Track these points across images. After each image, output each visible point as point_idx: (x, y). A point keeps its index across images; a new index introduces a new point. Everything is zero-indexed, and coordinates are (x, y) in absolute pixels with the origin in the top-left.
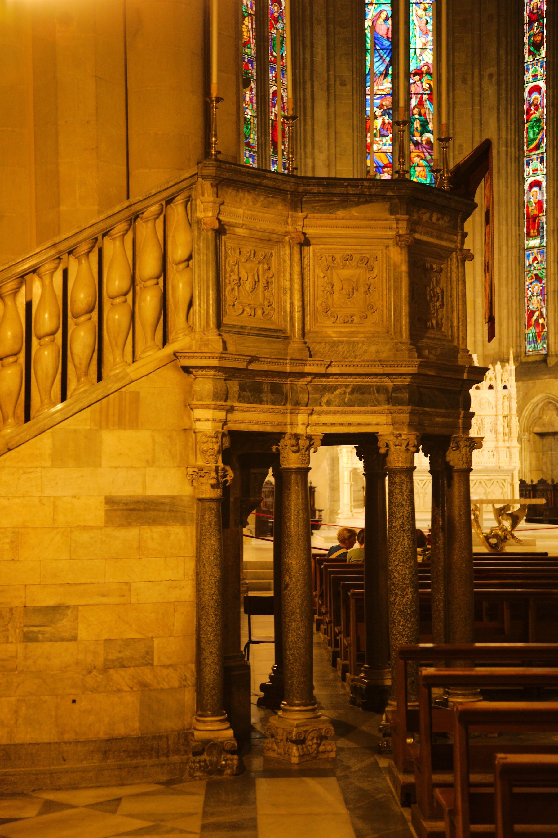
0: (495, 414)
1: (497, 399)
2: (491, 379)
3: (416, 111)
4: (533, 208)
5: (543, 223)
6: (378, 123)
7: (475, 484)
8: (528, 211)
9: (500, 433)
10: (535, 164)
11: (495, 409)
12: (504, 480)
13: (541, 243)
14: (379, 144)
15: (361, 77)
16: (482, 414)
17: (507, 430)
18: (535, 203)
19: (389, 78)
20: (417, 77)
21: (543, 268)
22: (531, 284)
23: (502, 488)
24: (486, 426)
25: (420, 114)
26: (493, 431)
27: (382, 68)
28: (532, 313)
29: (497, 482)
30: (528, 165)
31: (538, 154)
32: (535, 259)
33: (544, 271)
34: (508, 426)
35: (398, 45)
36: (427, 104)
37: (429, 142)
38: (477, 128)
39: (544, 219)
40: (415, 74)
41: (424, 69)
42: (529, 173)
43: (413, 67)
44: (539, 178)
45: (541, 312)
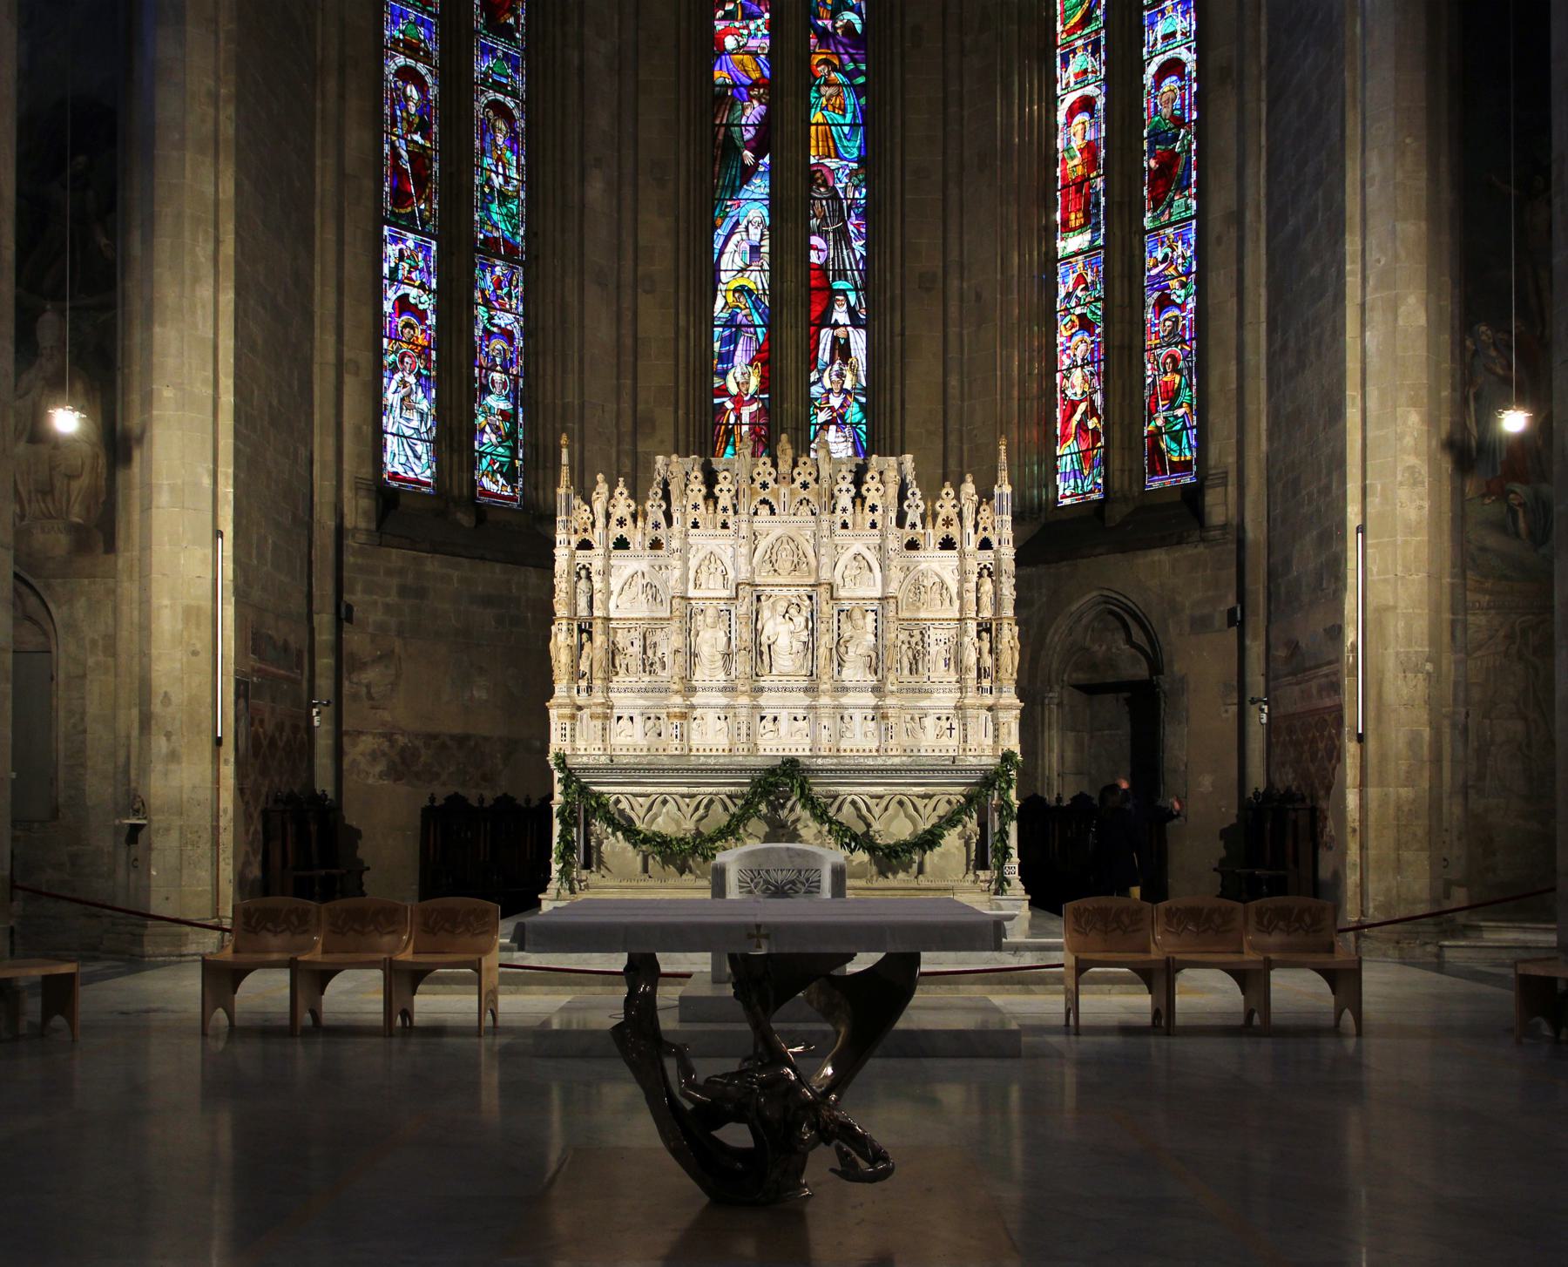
1: (963, 574)
2: (948, 522)
4: (1076, 162)
5: (1097, 194)
7: (886, 809)
8: (1064, 170)
9: (968, 669)
10: (1079, 62)
11: (957, 603)
13: (1092, 242)
14: (741, 35)
16: (922, 615)
17: (988, 661)
18: (1081, 151)
21: (1097, 299)
22: (1070, 338)
24: (933, 649)
28: (1074, 405)
30: (1065, 64)
31: (1088, 36)
32: (1080, 279)
33: (1099, 305)
34: (991, 652)
39: (1100, 184)
42: (1068, 84)
44: (1090, 90)
45: (1092, 402)
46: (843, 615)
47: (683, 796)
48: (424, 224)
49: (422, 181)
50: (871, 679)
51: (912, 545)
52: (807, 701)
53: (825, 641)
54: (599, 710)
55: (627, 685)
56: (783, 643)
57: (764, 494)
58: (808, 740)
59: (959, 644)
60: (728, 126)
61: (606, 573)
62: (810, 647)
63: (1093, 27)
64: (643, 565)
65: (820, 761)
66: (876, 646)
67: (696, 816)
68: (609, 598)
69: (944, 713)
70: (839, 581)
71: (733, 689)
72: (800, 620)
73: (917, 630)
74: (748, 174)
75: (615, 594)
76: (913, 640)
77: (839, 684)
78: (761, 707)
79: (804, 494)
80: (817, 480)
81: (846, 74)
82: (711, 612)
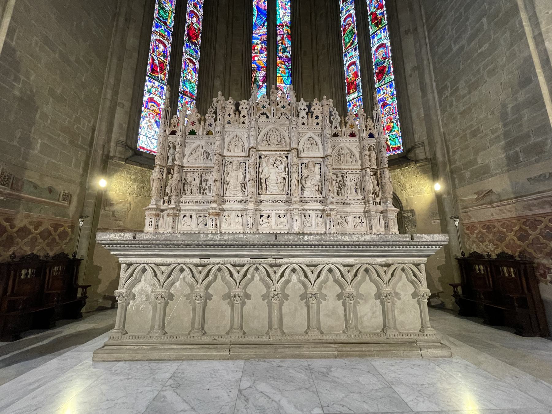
0: (360, 168)
1: (362, 149)
3: (280, 42)
5: (359, 83)
6: (259, 47)
7: (355, 275)
12: (417, 265)
15: (250, 27)
16: (342, 167)
19: (265, 27)
20: (281, 27)
23: (412, 282)
24: (349, 183)
25: (282, 44)
26: (359, 191)
27: (262, 23)
29: (403, 270)
35: (270, 13)
36: (286, 40)
37: (287, 57)
38: (314, 42)
39: (359, 80)
40: (279, 26)
41: (284, 24)
43: (278, 23)
46: (303, 166)
47: (196, 265)
48: (162, 80)
49: (162, 70)
50: (319, 197)
51: (336, 135)
52: (286, 207)
53: (295, 177)
54: (171, 211)
55: (190, 199)
56: (273, 177)
57: (264, 110)
58: (287, 228)
59: (363, 181)
60: (255, 76)
61: (183, 145)
62: (287, 180)
63: (354, 45)
64: (203, 143)
65: (306, 238)
66: (321, 181)
67: (205, 282)
68: (184, 157)
69: (357, 215)
70: (300, 149)
71: (246, 201)
72: (282, 167)
73: (340, 174)
74: (260, 87)
75: (187, 155)
76: (338, 179)
77: (303, 199)
78: (261, 210)
79: (283, 110)
80: (289, 104)
81: (286, 66)
82: (235, 163)
